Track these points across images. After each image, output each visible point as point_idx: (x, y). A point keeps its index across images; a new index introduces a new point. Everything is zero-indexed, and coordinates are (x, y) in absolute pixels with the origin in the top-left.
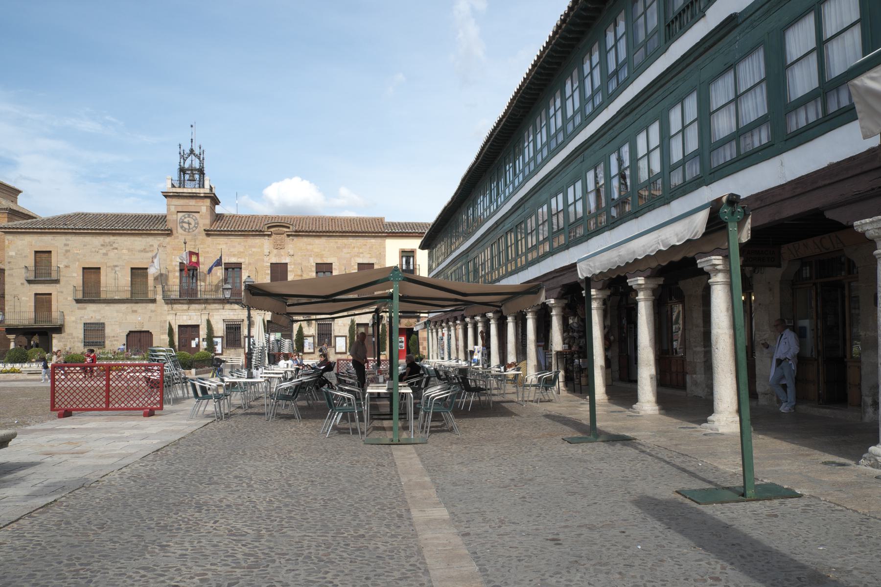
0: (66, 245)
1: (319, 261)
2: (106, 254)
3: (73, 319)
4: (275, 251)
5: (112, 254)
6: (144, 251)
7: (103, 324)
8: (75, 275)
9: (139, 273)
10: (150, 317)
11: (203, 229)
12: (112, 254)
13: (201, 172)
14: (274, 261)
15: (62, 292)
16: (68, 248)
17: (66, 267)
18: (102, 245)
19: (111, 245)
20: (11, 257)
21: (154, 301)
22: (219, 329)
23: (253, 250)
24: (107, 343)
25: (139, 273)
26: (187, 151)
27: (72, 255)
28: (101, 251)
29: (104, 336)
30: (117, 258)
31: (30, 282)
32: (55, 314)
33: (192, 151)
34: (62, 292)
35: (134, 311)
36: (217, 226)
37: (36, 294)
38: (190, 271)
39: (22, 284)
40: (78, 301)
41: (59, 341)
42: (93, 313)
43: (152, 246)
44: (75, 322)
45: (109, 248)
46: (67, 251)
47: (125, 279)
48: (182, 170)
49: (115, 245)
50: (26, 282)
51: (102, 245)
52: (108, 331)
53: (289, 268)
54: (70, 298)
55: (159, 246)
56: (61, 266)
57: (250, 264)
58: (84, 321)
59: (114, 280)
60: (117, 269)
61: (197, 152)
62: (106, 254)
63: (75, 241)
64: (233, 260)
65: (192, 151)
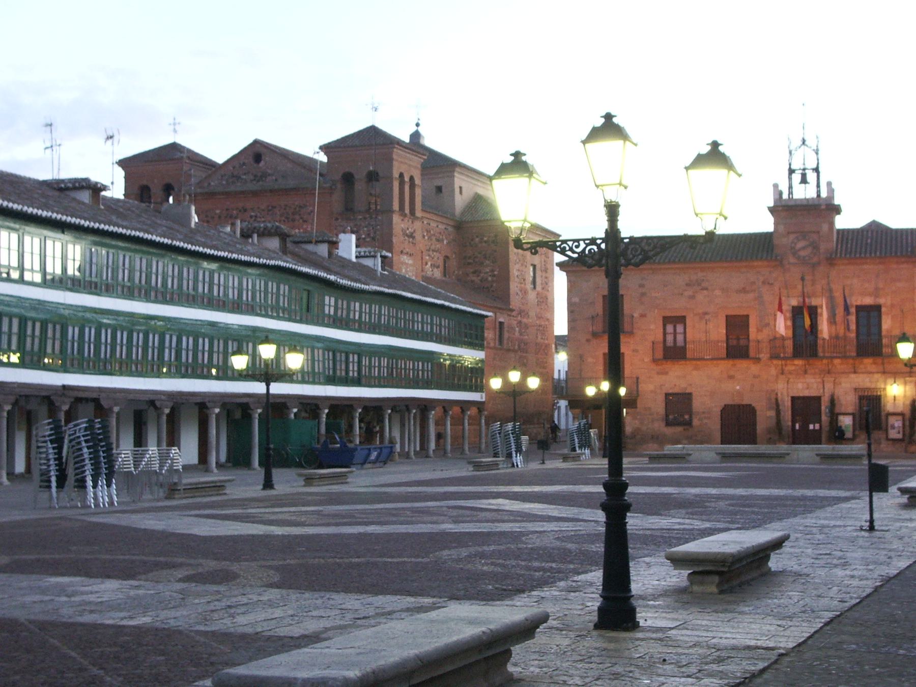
0: (642, 286)
2: (692, 297)
3: (651, 387)
5: (700, 297)
6: (744, 291)
7: (690, 394)
8: (652, 327)
9: (737, 325)
10: (753, 385)
13: (816, 170)
17: (643, 316)
18: (687, 285)
19: (699, 285)
21: (758, 360)
23: (899, 285)
24: (696, 422)
25: (737, 325)
28: (686, 293)
29: (691, 414)
35: (731, 377)
39: (588, 340)
40: (655, 361)
42: (677, 377)
43: (754, 283)
46: (643, 294)
47: (718, 331)
48: (791, 171)
49: (704, 285)
52: (697, 404)
55: (764, 283)
56: (635, 315)
57: (892, 306)
58: (664, 391)
60: (707, 317)
62: (692, 297)
64: (868, 301)
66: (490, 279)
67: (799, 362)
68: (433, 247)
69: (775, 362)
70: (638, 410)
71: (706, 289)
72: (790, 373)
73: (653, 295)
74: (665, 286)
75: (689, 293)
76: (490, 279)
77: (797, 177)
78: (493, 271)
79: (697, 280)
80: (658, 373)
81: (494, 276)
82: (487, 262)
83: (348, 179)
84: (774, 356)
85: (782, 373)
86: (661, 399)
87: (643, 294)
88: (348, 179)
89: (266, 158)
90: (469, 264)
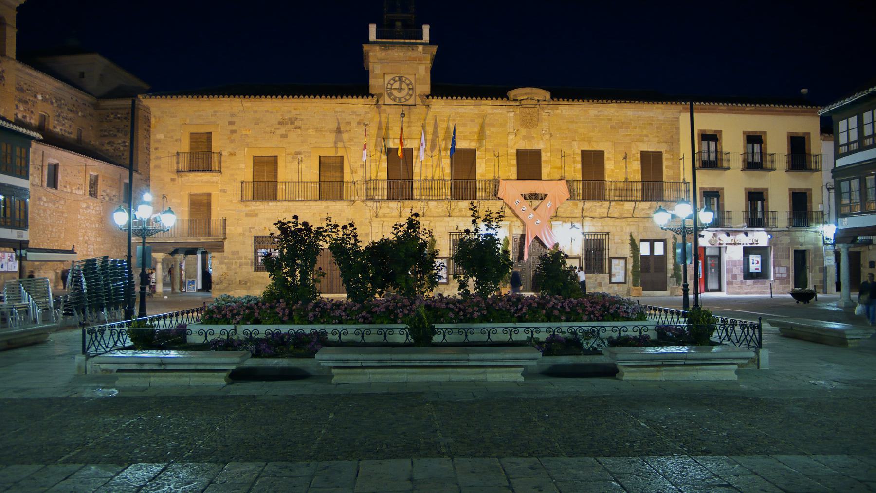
1: (587, 148)
2: (284, 136)
3: (240, 230)
4: (523, 131)
8: (242, 166)
14: (524, 145)
15: (225, 191)
16: (234, 128)
17: (231, 154)
18: (280, 123)
19: (292, 123)
20: (159, 141)
28: (279, 132)
32: (215, 225)
34: (225, 191)
37: (191, 195)
39: (173, 180)
41: (221, 263)
44: (243, 234)
45: (289, 126)
47: (311, 172)
49: (297, 123)
50: (175, 176)
51: (280, 123)
53: (544, 157)
60: (299, 157)
66: (122, 148)
67: (393, 205)
68: (65, 115)
69: (370, 204)
70: (225, 254)
71: (300, 128)
72: (385, 216)
73: (244, 133)
74: (257, 124)
75: (282, 131)
76: (122, 148)
78: (124, 142)
79: (290, 119)
80: (247, 215)
81: (125, 146)
82: (120, 135)
84: (369, 198)
85: (377, 216)
86: (250, 242)
87: (233, 132)
90: (105, 136)
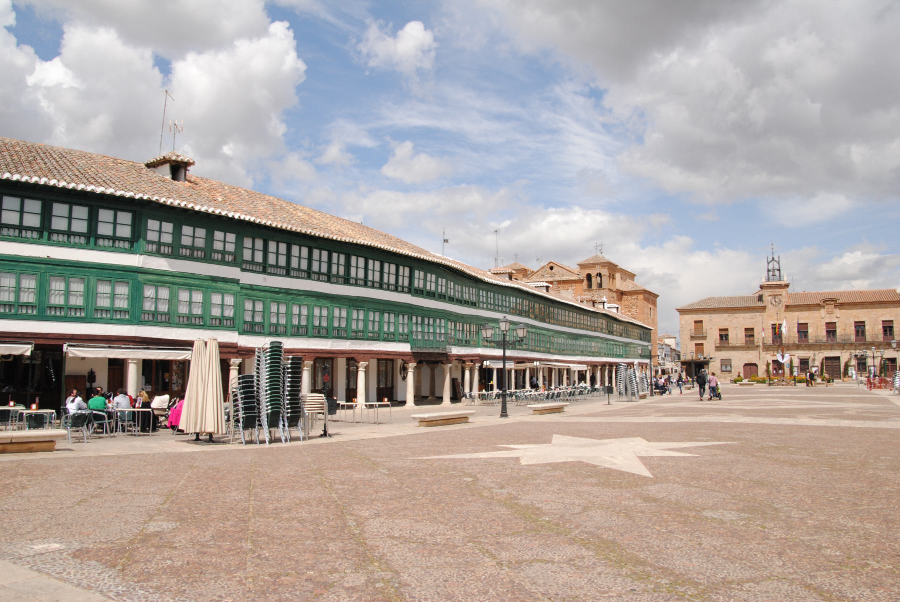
5: (734, 321)
6: (752, 318)
9: (749, 332)
11: (784, 304)
12: (734, 321)
13: (779, 270)
22: (796, 362)
25: (749, 332)
26: (770, 259)
27: (713, 324)
30: (736, 325)
31: (692, 338)
33: (773, 259)
36: (791, 303)
38: (776, 331)
42: (725, 354)
48: (769, 271)
54: (713, 346)
59: (737, 336)
61: (776, 259)
63: (716, 317)
65: (773, 259)
77: (771, 273)
83: (589, 277)
88: (589, 277)
89: (555, 268)
